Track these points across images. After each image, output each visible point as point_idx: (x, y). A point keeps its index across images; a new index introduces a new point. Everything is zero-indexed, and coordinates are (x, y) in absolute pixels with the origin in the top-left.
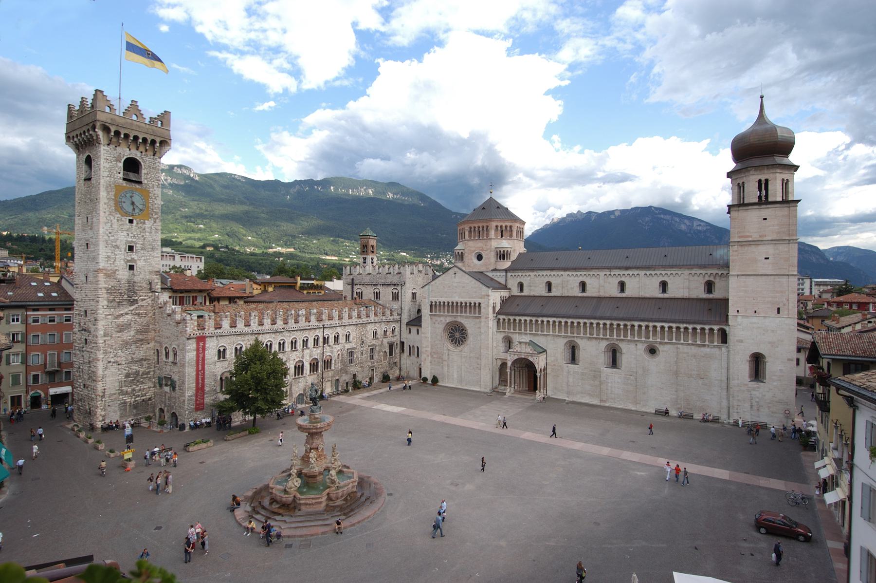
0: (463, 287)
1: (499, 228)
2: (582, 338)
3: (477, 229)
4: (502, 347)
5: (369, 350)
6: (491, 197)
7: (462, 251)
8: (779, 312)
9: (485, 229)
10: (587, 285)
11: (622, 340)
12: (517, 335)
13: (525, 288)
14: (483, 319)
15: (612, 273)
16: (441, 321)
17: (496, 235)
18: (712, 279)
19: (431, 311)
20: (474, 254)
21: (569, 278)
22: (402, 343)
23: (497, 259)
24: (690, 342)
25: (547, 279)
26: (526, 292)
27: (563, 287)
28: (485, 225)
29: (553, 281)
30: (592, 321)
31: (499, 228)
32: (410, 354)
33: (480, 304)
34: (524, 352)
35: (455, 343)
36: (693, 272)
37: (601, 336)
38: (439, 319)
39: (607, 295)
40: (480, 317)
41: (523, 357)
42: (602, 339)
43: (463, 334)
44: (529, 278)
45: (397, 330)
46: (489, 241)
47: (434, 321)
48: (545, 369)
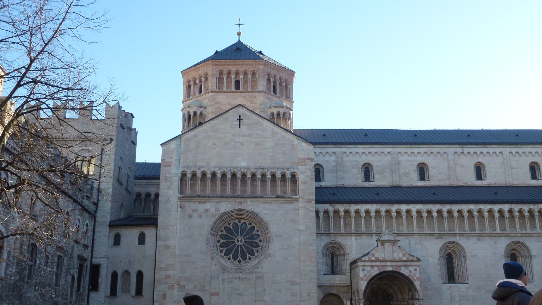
0: (257, 144)
1: (272, 80)
2: (467, 236)
3: (233, 76)
4: (324, 263)
5: (56, 259)
6: (239, 41)
7: (202, 110)
9: (250, 76)
10: (430, 169)
11: (530, 235)
12: (353, 238)
14: (301, 204)
15: (466, 150)
16: (206, 210)
17: (268, 89)
19: (181, 191)
21: (401, 158)
22: (95, 269)
25: (364, 159)
26: (329, 181)
27: (392, 171)
29: (375, 161)
30: (482, 206)
31: (272, 80)
32: (113, 292)
33: (293, 176)
34: (391, 259)
35: (235, 258)
37: (498, 231)
38: (201, 207)
39: (461, 183)
40: (297, 199)
41: (390, 269)
42: (500, 235)
43: (252, 238)
44: (333, 158)
45: (90, 234)
46: (257, 94)
47: (189, 211)
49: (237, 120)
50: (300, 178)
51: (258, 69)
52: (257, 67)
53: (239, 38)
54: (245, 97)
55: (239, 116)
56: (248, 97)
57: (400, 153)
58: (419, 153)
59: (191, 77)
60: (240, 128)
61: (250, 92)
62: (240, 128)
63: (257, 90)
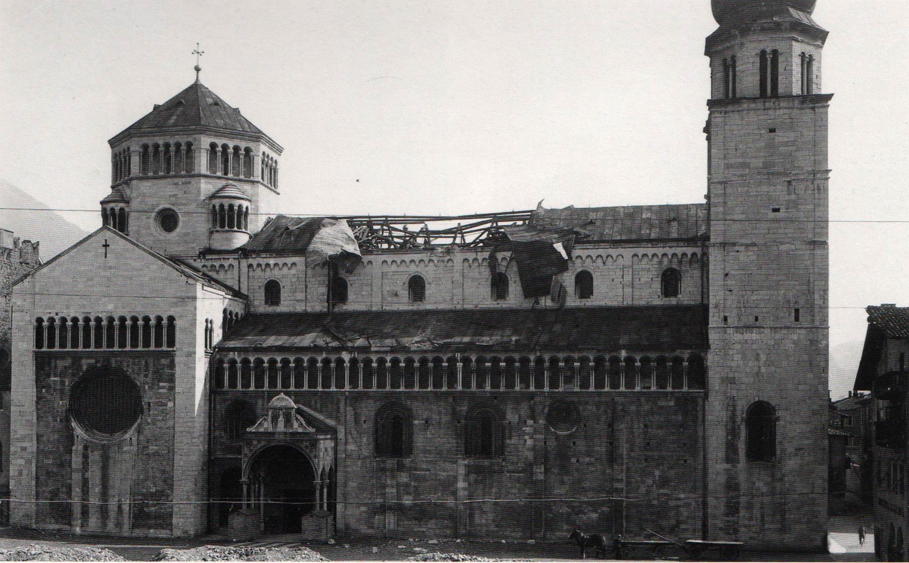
7: (122, 205)
8: (797, 319)
13: (284, 295)
18: (674, 266)
20: (153, 215)
21: (386, 269)
23: (214, 225)
24: (638, 389)
28: (183, 139)
33: (171, 319)
36: (641, 251)
44: (293, 271)
48: (333, 472)
49: (104, 246)
50: (178, 323)
51: (195, 139)
52: (193, 136)
53: (197, 77)
54: (176, 184)
55: (104, 241)
56: (180, 183)
57: (385, 262)
58: (412, 261)
59: (117, 149)
60: (106, 257)
61: (183, 177)
62: (106, 257)
63: (193, 172)
